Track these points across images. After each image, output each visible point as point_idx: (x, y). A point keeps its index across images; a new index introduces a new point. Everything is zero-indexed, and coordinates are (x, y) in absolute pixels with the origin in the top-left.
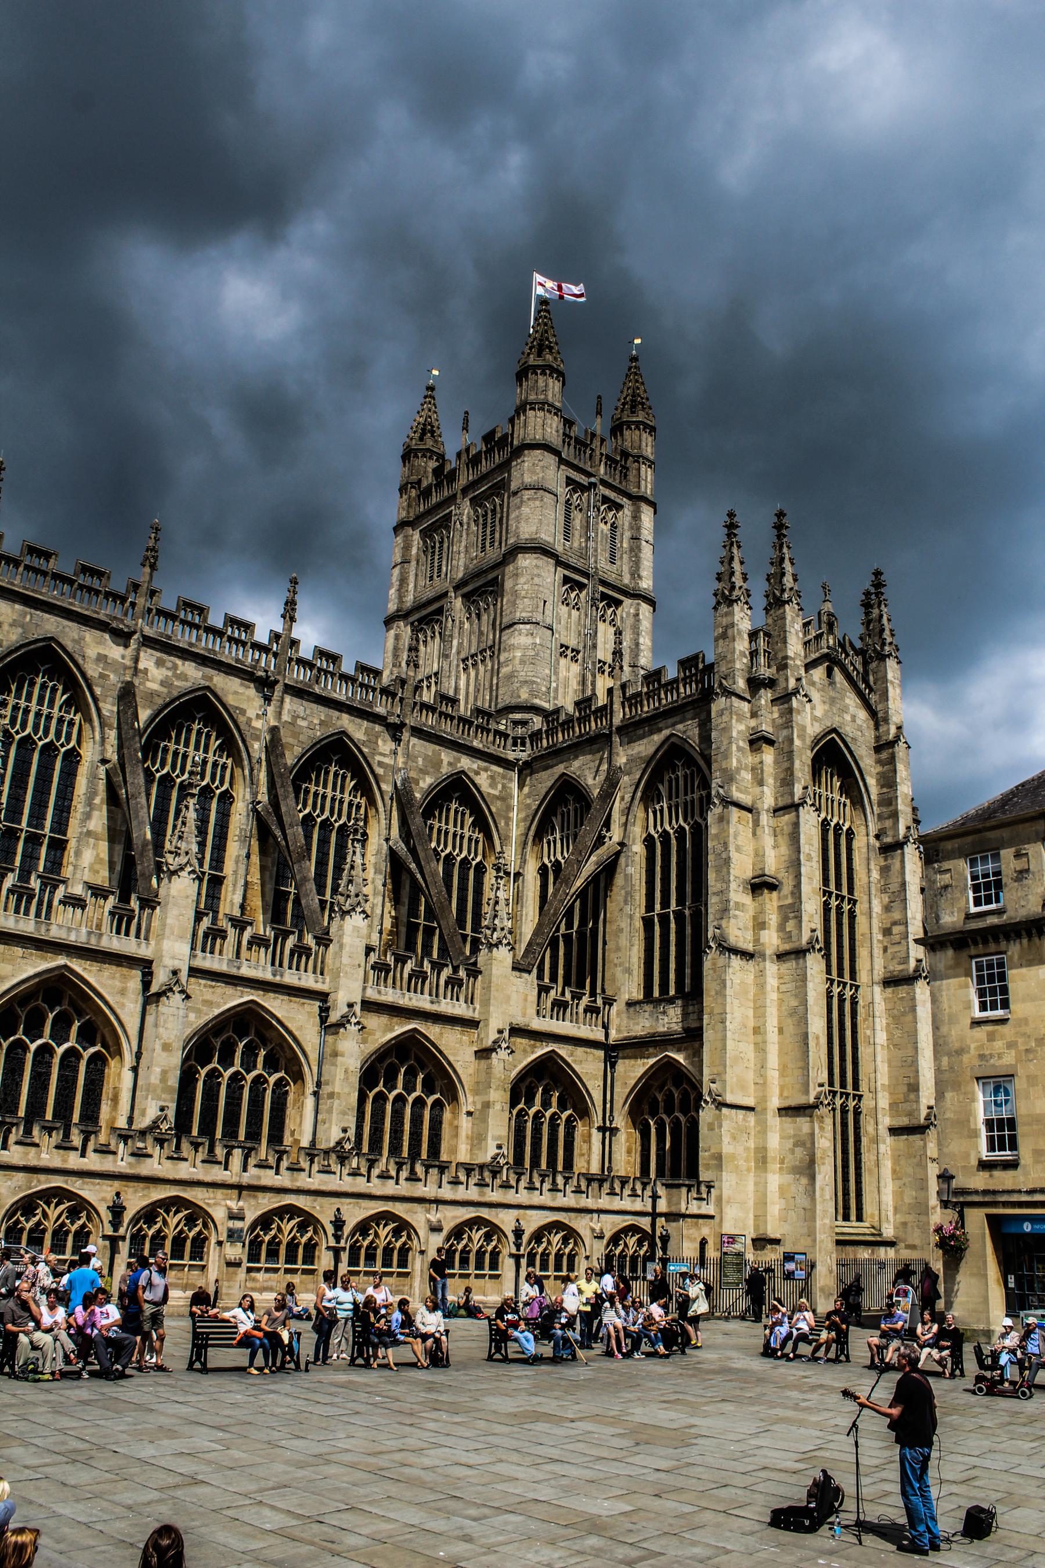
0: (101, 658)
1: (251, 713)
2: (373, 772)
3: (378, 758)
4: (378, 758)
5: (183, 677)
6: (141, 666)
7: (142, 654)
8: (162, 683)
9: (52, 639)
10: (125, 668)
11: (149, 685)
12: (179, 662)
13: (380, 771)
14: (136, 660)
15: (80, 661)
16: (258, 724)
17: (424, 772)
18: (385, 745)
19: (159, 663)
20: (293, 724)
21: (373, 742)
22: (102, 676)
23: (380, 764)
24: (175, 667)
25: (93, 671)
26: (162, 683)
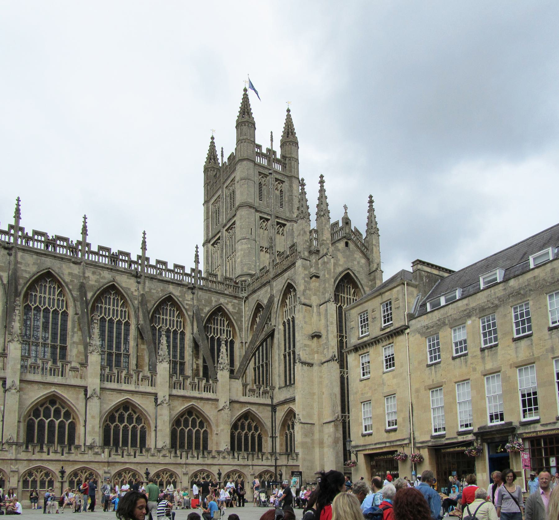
0: (70, 274)
1: (133, 289)
2: (184, 308)
3: (186, 302)
4: (186, 302)
5: (104, 278)
6: (86, 275)
7: (86, 271)
8: (96, 281)
9: (49, 268)
10: (80, 277)
11: (90, 282)
12: (102, 272)
13: (187, 307)
14: (84, 273)
15: (62, 276)
16: (136, 293)
17: (205, 306)
18: (189, 296)
19: (94, 273)
20: (150, 292)
21: (183, 296)
22: (71, 281)
23: (187, 304)
24: (100, 274)
25: (67, 279)
26: (96, 281)
